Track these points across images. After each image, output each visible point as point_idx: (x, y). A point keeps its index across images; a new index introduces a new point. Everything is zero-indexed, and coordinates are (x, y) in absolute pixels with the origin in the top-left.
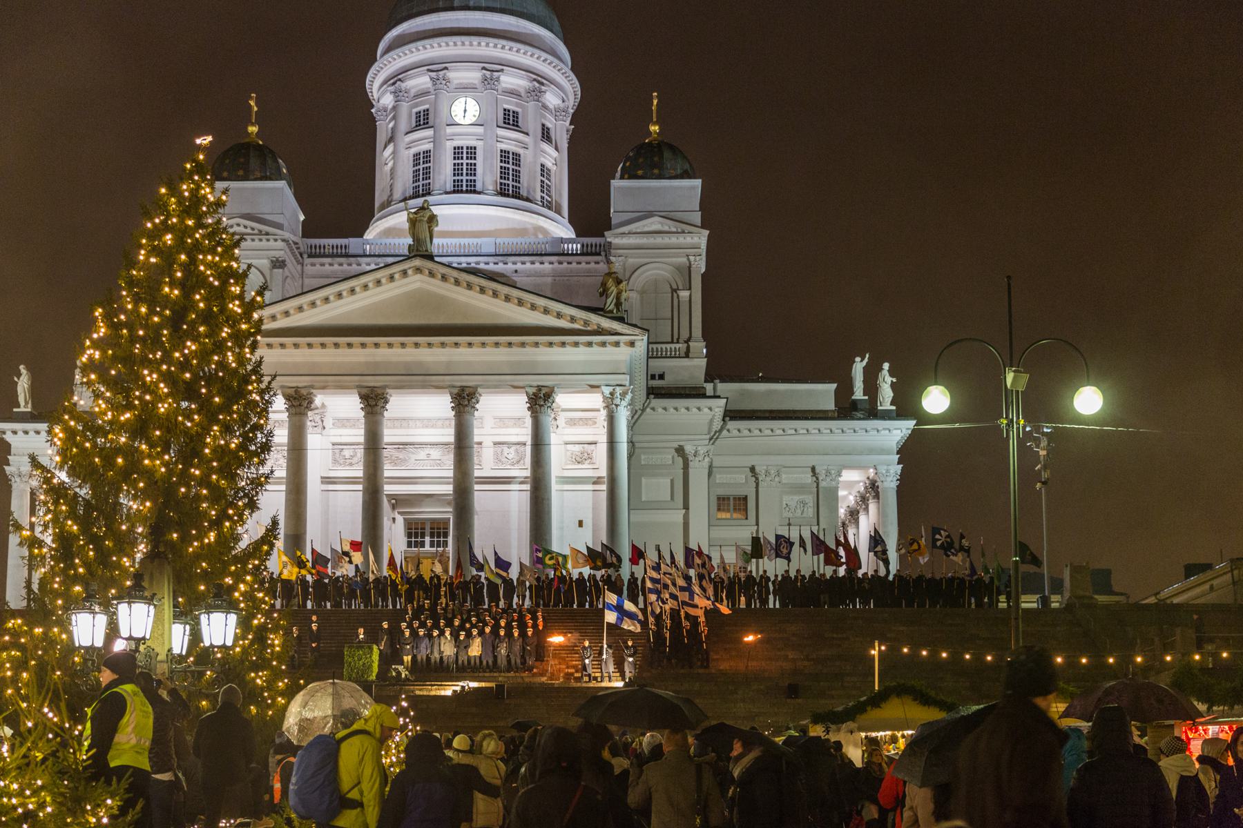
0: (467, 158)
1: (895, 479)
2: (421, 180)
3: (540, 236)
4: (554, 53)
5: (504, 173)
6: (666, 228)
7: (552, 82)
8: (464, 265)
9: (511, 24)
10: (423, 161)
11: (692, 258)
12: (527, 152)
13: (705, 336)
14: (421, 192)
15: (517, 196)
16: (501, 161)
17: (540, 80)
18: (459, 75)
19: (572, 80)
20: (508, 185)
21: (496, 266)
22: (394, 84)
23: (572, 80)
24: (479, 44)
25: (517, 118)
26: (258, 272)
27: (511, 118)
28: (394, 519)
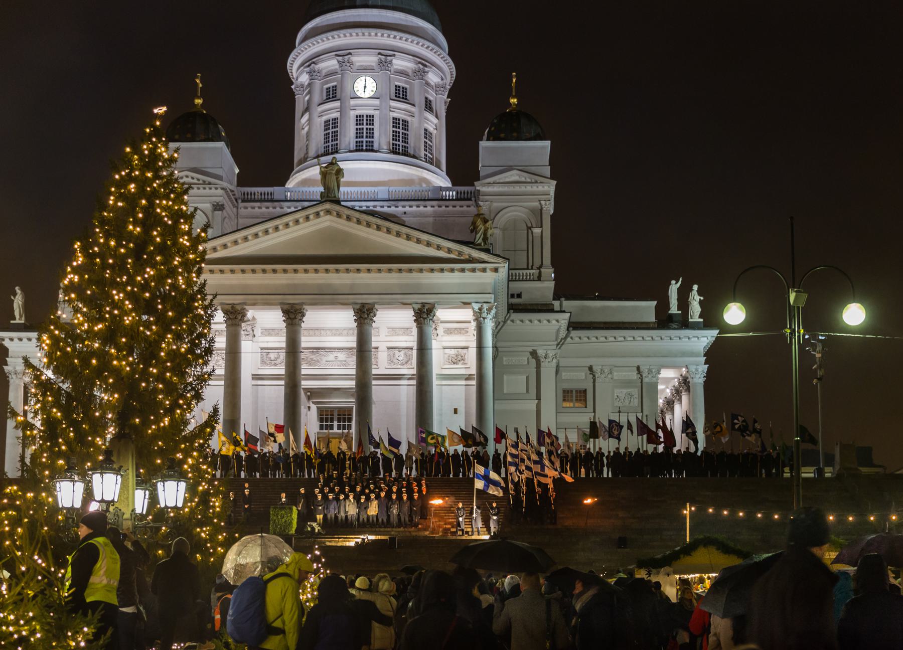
0: (367, 124)
1: (702, 376)
2: (330, 141)
3: (424, 185)
4: (434, 41)
5: (395, 136)
6: (523, 179)
7: (433, 64)
8: (364, 208)
9: (401, 19)
10: (332, 125)
11: (543, 203)
12: (413, 119)
13: (553, 264)
14: (330, 151)
15: (406, 154)
16: (393, 127)
17: (424, 63)
18: (361, 59)
19: (449, 63)
20: (399, 145)
21: (389, 209)
22: (309, 66)
23: (449, 63)
24: (376, 35)
25: (406, 92)
26: (203, 215)
27: (401, 93)
28: (309, 408)
